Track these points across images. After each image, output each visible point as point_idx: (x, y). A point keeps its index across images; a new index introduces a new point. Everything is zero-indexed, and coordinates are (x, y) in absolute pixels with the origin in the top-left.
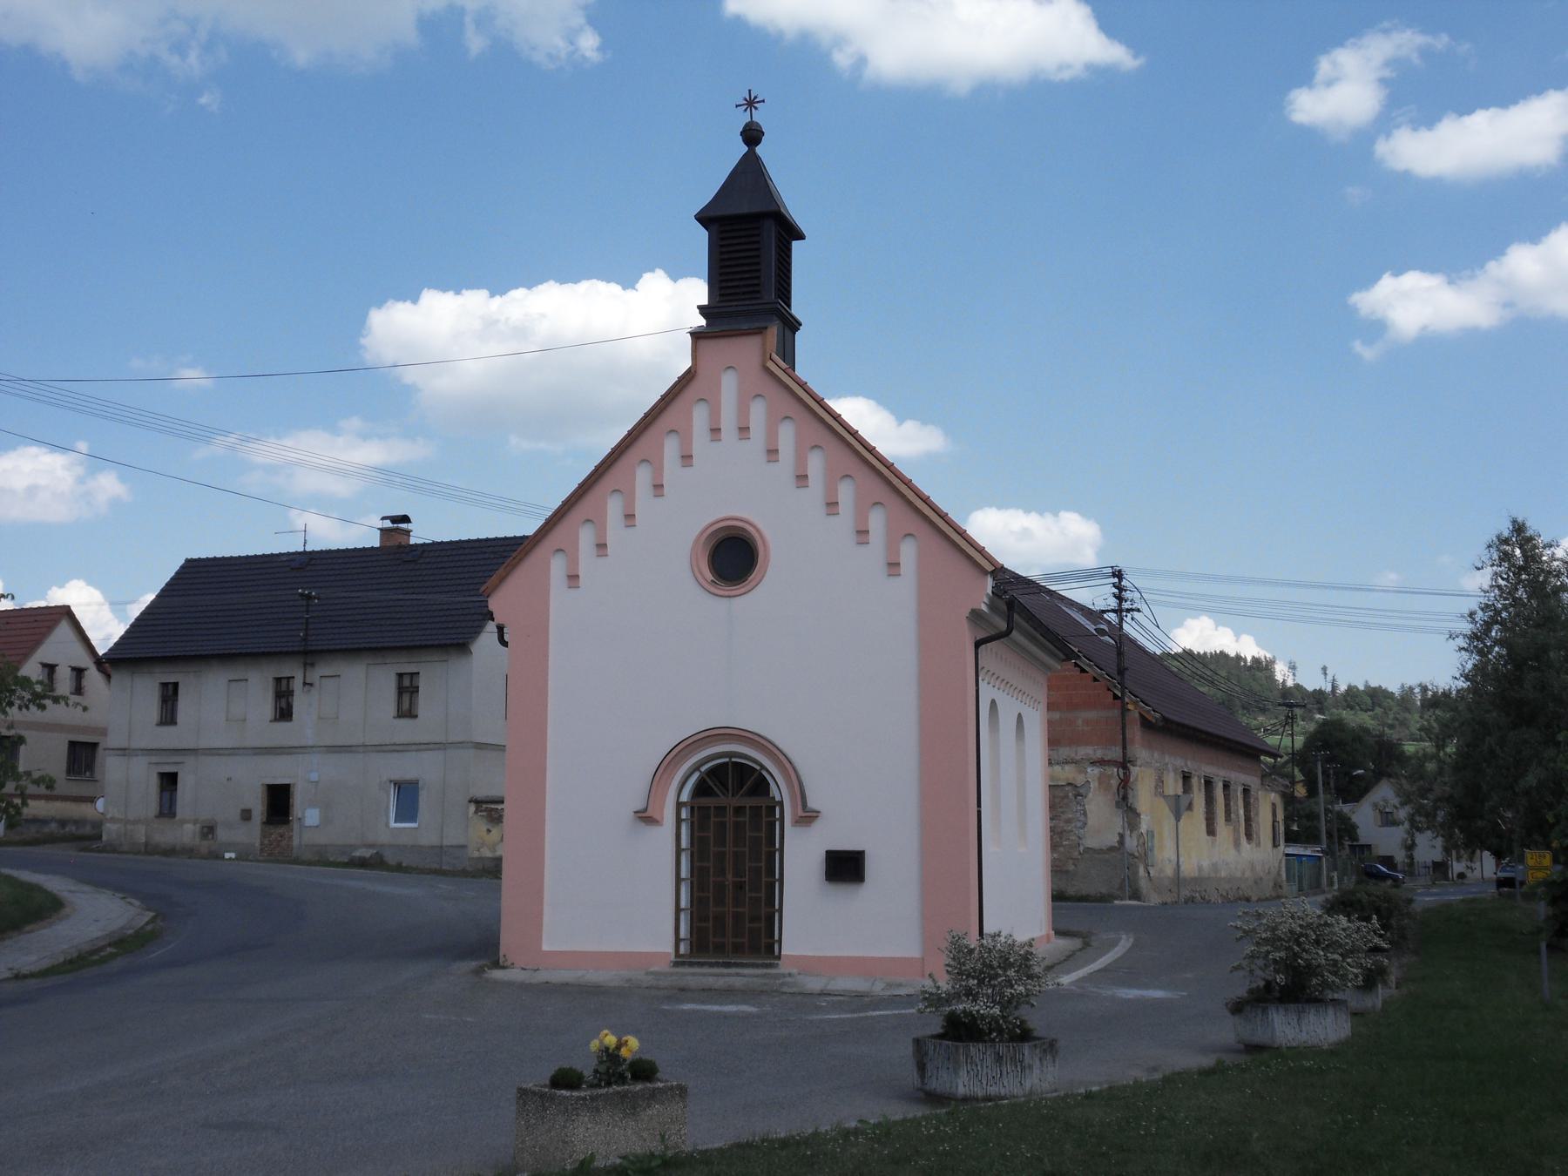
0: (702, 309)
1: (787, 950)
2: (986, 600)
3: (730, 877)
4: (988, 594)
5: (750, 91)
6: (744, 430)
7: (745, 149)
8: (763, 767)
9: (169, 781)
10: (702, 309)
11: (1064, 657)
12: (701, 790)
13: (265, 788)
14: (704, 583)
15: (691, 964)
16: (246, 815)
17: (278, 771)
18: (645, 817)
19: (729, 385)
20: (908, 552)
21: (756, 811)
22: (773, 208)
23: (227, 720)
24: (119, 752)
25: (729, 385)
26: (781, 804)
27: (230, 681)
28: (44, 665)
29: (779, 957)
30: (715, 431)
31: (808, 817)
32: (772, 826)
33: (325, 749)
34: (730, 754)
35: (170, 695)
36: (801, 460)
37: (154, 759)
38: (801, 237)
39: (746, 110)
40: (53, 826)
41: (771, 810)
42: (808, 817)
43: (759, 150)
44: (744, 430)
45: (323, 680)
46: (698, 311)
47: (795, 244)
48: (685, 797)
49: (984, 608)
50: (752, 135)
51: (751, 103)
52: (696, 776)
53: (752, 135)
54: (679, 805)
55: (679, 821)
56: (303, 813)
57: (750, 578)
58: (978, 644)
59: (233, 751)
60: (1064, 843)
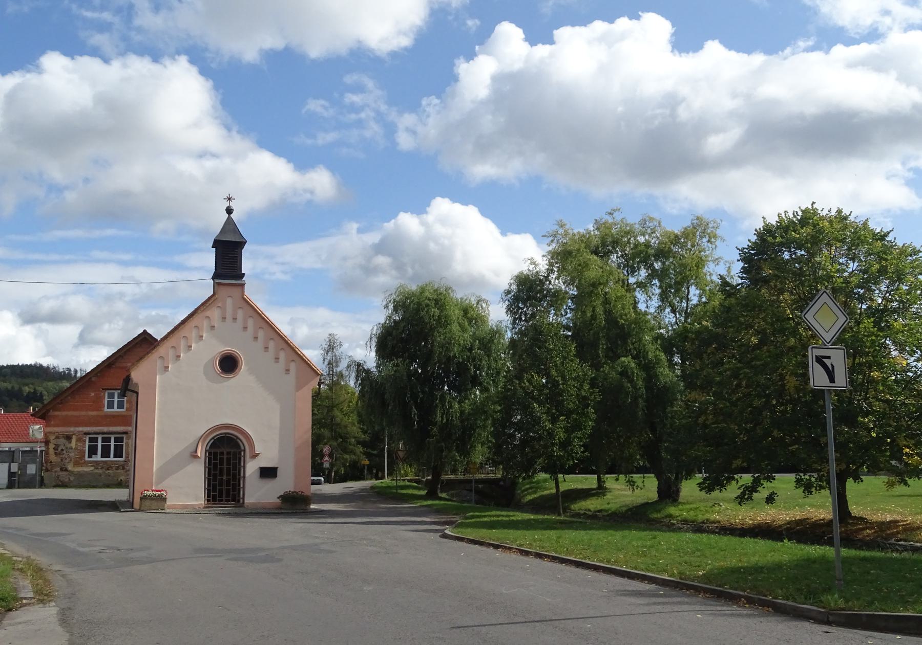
1: (248, 501)
6: (235, 319)
7: (227, 215)
8: (238, 438)
18: (194, 455)
20: (293, 366)
21: (235, 453)
25: (229, 301)
26: (244, 451)
29: (243, 503)
30: (224, 318)
31: (254, 456)
32: (240, 459)
41: (240, 453)
42: (254, 456)
43: (232, 216)
44: (235, 319)
48: (208, 448)
50: (229, 211)
51: (229, 199)
53: (229, 211)
54: (206, 451)
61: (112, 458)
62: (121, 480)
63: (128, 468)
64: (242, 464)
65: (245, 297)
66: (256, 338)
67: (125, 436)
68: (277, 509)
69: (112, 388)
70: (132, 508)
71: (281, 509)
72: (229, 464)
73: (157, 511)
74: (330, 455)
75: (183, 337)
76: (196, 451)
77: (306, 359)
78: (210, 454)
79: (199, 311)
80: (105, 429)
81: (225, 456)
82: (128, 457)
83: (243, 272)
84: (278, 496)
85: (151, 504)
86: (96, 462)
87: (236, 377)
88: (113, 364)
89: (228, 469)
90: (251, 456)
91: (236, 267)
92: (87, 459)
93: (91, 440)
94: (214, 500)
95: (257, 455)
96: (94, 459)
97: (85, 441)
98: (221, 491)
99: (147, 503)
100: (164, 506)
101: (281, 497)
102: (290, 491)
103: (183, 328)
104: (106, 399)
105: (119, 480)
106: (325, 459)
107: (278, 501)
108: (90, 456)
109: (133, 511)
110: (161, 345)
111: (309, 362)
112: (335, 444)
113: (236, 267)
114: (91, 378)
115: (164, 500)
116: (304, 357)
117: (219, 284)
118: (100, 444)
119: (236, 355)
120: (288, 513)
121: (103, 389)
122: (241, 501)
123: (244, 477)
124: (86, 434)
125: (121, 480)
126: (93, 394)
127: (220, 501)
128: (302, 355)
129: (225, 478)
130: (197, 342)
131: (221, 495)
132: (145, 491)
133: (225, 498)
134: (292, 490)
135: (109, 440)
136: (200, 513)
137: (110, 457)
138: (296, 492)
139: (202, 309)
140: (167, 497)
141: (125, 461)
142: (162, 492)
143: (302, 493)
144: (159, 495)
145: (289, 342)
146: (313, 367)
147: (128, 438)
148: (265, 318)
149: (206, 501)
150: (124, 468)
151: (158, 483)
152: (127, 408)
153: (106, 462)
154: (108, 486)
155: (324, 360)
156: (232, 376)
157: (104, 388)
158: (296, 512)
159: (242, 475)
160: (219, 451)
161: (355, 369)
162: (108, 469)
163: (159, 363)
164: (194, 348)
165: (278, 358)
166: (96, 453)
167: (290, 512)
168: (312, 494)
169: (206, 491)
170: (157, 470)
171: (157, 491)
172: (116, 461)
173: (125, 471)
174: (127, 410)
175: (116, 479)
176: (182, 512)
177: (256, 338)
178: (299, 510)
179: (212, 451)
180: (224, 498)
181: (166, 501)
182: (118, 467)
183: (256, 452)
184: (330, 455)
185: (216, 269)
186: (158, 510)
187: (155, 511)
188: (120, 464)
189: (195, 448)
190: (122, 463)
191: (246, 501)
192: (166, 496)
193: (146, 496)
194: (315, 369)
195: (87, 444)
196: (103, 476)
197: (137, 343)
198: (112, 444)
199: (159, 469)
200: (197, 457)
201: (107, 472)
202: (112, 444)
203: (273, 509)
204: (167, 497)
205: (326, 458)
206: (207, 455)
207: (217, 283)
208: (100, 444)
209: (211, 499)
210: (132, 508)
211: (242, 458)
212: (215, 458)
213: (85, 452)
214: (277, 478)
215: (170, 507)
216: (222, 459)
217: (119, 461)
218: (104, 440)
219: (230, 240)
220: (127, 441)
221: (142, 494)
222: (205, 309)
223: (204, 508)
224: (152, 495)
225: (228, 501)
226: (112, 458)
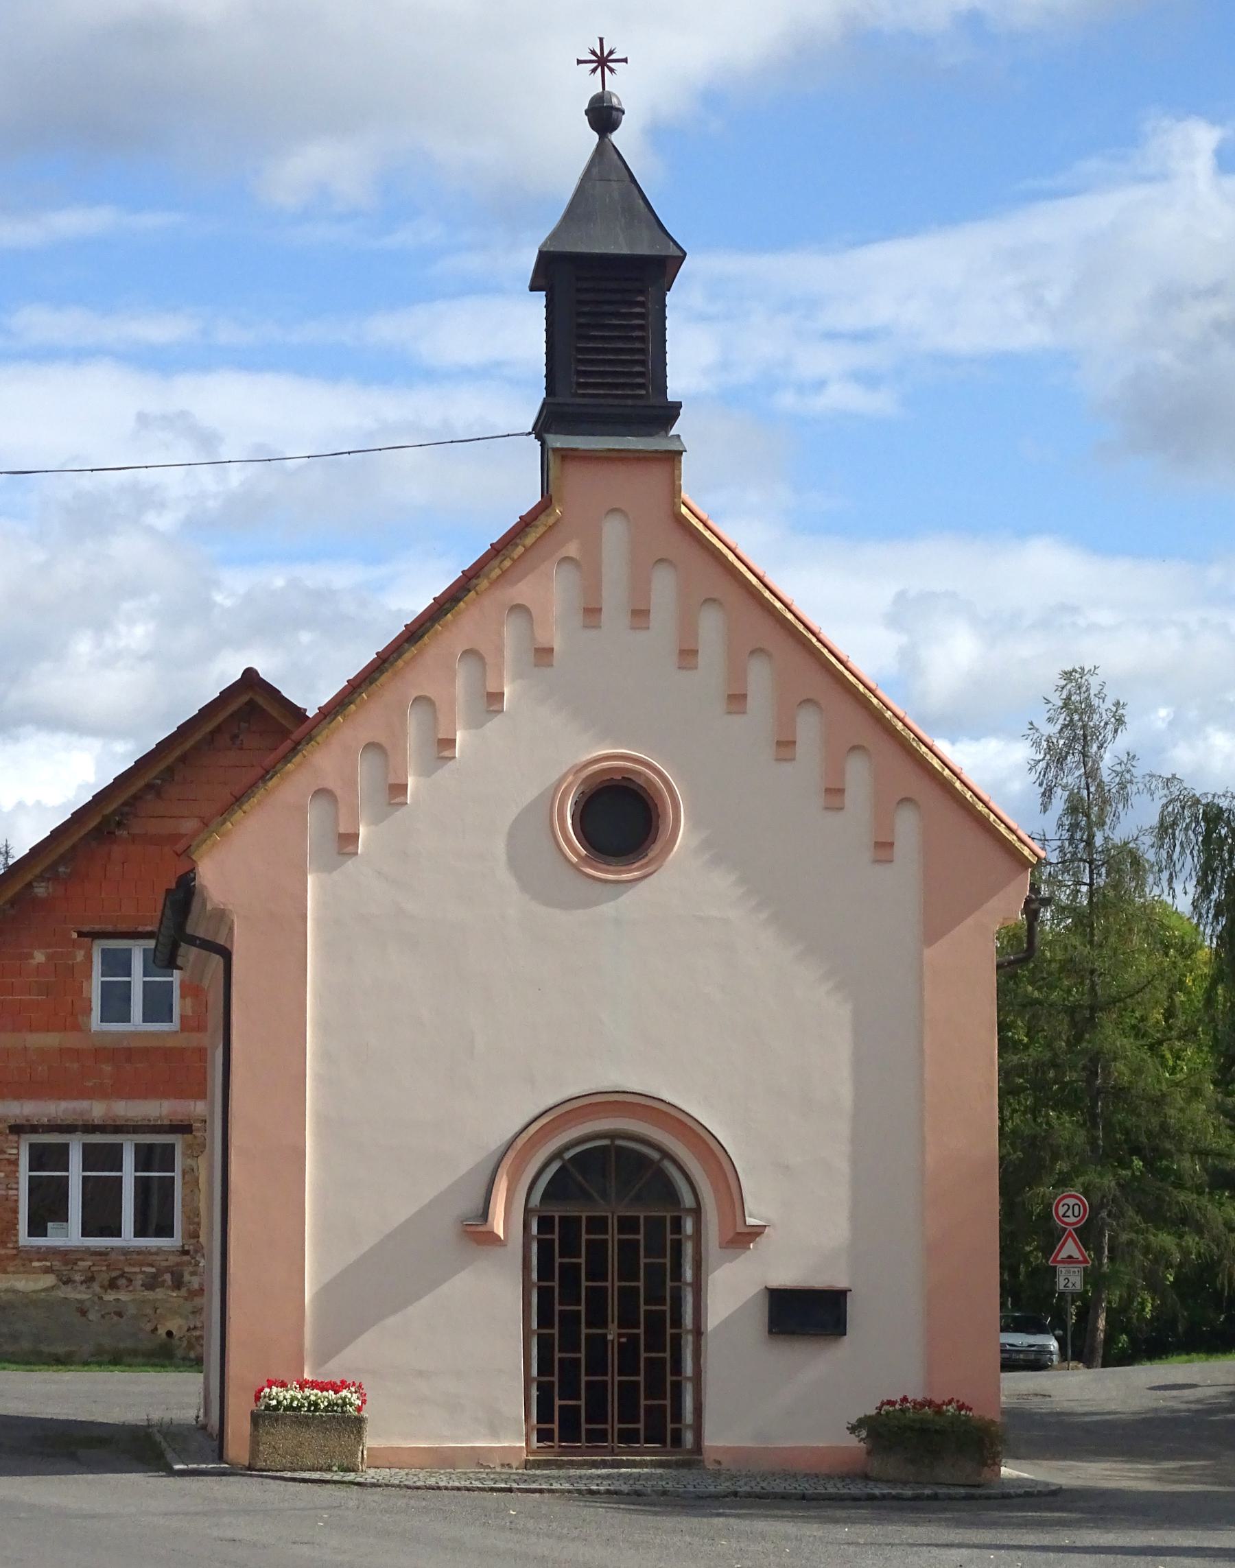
5: (601, 40)
6: (640, 615)
7: (595, 137)
8: (666, 1154)
12: (560, 1188)
14: (575, 860)
19: (614, 534)
20: (907, 827)
21: (655, 1225)
25: (614, 534)
26: (697, 1212)
30: (592, 613)
32: (677, 1248)
34: (612, 1135)
36: (736, 672)
39: (594, 70)
41: (677, 1225)
44: (640, 615)
51: (602, 61)
52: (555, 1166)
54: (527, 1211)
57: (651, 854)
61: (128, 1237)
62: (169, 1334)
63: (195, 1283)
64: (688, 1275)
65: (684, 510)
66: (737, 700)
67: (177, 1141)
69: (123, 927)
70: (221, 1458)
71: (866, 1477)
72: (628, 1270)
73: (328, 1476)
74: (1087, 1234)
75: (416, 699)
76: (485, 1214)
77: (969, 795)
78: (545, 1224)
79: (484, 583)
80: (97, 1110)
81: (613, 1237)
82: (195, 1235)
83: (671, 397)
84: (854, 1421)
85: (300, 1444)
86: (67, 1256)
87: (646, 881)
88: (119, 824)
89: (628, 1296)
90: (731, 1235)
91: (641, 374)
92: (24, 1239)
93: (40, 1157)
94: (570, 1431)
95: (755, 1233)
96: (54, 1238)
97: (15, 1163)
98: (597, 1393)
99: (282, 1438)
100: (353, 1454)
102: (905, 1399)
103: (414, 657)
104: (97, 979)
105: (162, 1332)
106: (1063, 1254)
107: (854, 1443)
108: (37, 1228)
109: (223, 1473)
110: (319, 739)
111: (980, 806)
112: (1109, 1182)
113: (641, 374)
114: (29, 885)
115: (356, 1424)
116: (958, 785)
117: (566, 455)
118: (75, 1174)
119: (648, 780)
120: (897, 1498)
121: (81, 934)
122: (688, 1437)
123: (698, 1332)
124: (17, 1129)
125: (169, 1334)
126: (39, 957)
128: (947, 772)
129: (612, 1333)
130: (475, 724)
131: (597, 1412)
132: (270, 1384)
133: (617, 1426)
134: (916, 1394)
135: (112, 1157)
136: (510, 1490)
137: (118, 1233)
138: (929, 1403)
139: (497, 572)
140: (364, 1414)
141: (186, 1253)
142: (344, 1393)
143: (961, 1407)
144: (331, 1404)
145: (888, 714)
146: (1002, 828)
147: (196, 1150)
148: (778, 605)
149: (534, 1437)
150: (178, 1284)
151: (323, 1358)
152: (182, 1017)
153: (102, 1253)
154: (115, 1359)
155: (1048, 794)
157: (86, 929)
158: (935, 1497)
159: (688, 1321)
160: (584, 1215)
161: (1196, 839)
162: (112, 1285)
163: (314, 816)
164: (462, 752)
165: (840, 791)
166: (63, 1217)
167: (909, 1492)
168: (1005, 1412)
169: (534, 1393)
170: (317, 1296)
171: (323, 1387)
172: (140, 1252)
173: (183, 1292)
174: (184, 1027)
175: (149, 1327)
176: (432, 1481)
179: (557, 1212)
180: (614, 1425)
181: (360, 1433)
182: (155, 1276)
183: (751, 1221)
184: (1087, 1234)
185: (550, 389)
186: (329, 1469)
187: (316, 1475)
188: (164, 1264)
190: (173, 1259)
191: (709, 1442)
192: (359, 1409)
193: (276, 1408)
194: (1012, 837)
195: (24, 1174)
196: (92, 1316)
197: (218, 729)
198: (128, 1174)
199: (327, 1292)
201: (110, 1296)
202: (128, 1174)
203: (829, 1477)
204: (364, 1414)
205: (1070, 1248)
206: (534, 1229)
207: (556, 450)
208: (75, 1174)
209: (555, 1426)
210: (221, 1458)
211: (688, 1248)
212: (570, 1247)
213: (15, 1211)
214: (845, 1337)
215: (380, 1458)
216: (596, 1250)
217: (159, 1251)
218: (92, 1157)
219: (613, 250)
220: (189, 1161)
221: (257, 1398)
222: (504, 573)
223: (527, 1464)
224: (299, 1408)
225: (628, 1437)
226: (128, 1237)
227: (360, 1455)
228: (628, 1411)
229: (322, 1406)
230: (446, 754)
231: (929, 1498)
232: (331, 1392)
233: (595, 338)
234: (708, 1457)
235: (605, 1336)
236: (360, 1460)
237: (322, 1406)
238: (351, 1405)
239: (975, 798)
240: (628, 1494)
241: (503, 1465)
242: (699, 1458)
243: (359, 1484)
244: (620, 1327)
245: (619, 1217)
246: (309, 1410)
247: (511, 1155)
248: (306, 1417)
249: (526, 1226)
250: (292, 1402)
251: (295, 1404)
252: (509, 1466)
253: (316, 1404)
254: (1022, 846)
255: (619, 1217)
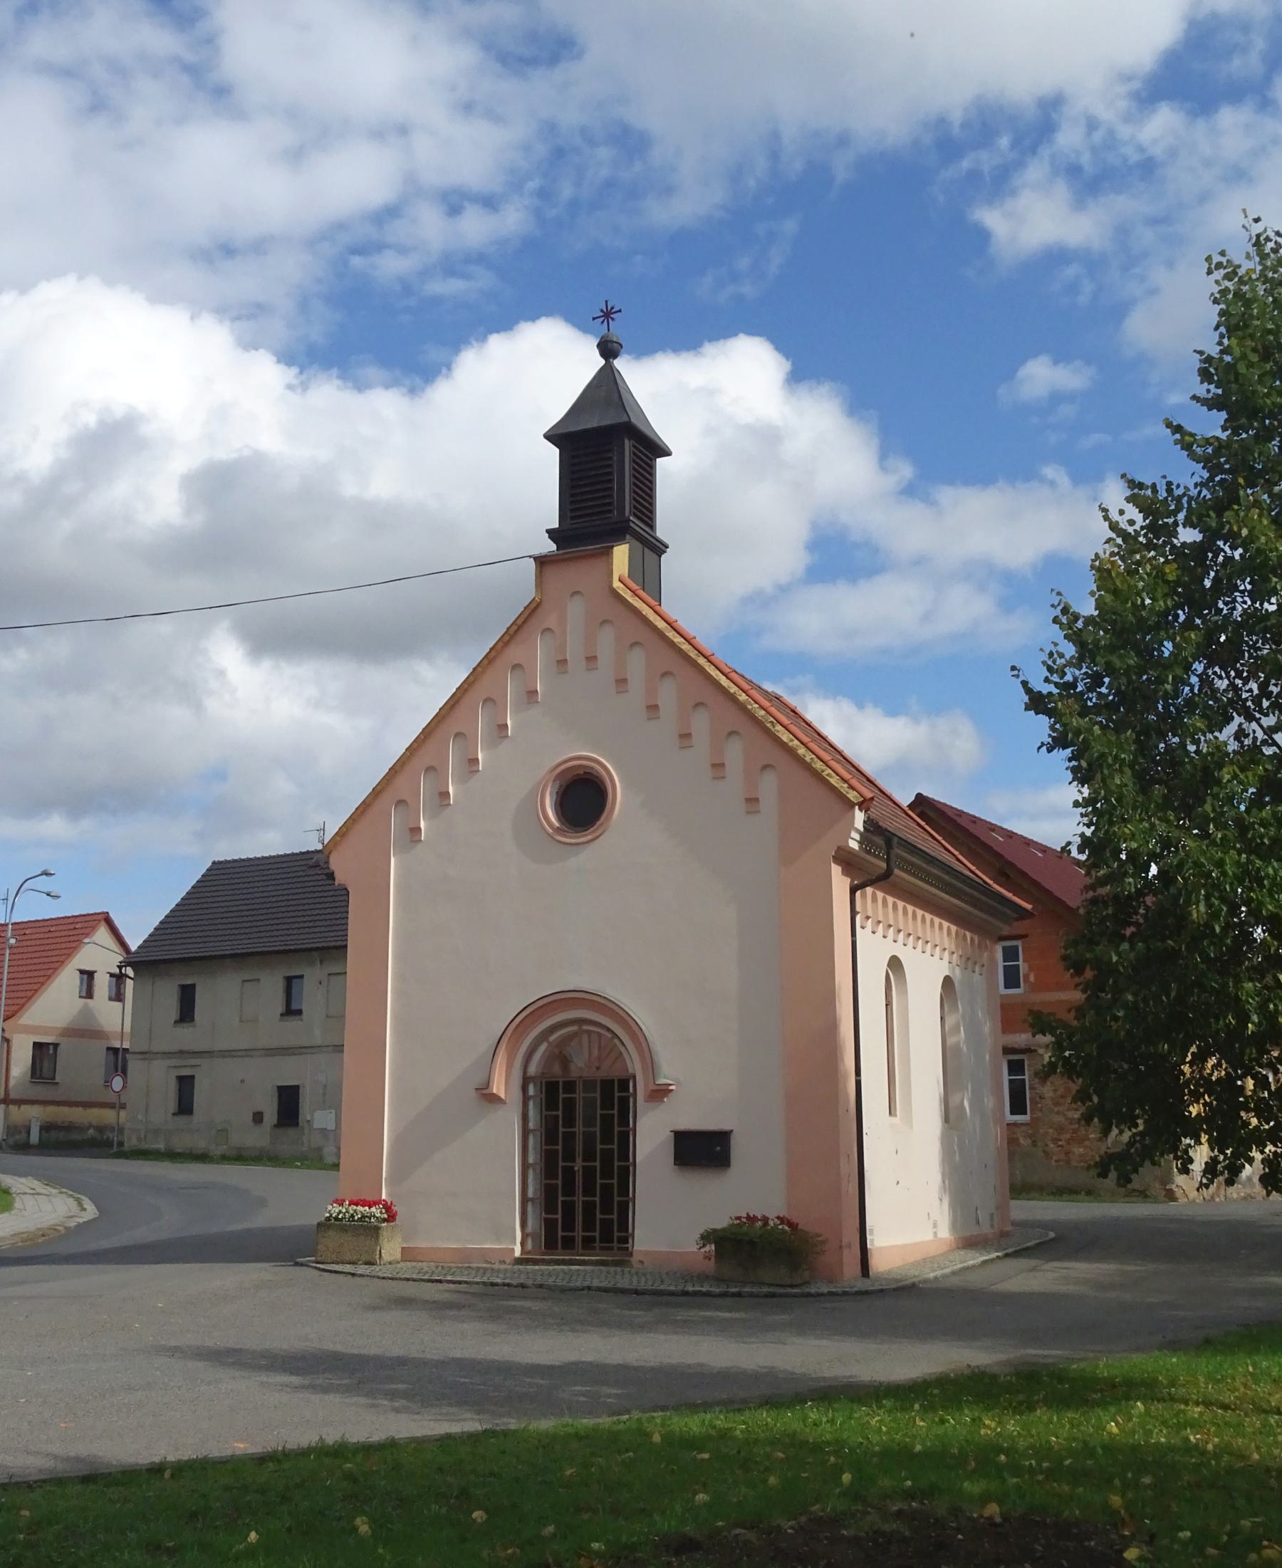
0: (552, 533)
2: (857, 837)
3: (578, 1165)
4: (857, 831)
6: (591, 659)
9: (185, 1085)
10: (552, 533)
11: (1015, 915)
13: (276, 1089)
14: (551, 831)
15: (535, 1262)
16: (258, 1117)
17: (288, 1072)
19: (576, 610)
20: (768, 786)
21: (607, 1085)
22: (625, 419)
23: (241, 1021)
24: (140, 1056)
26: (634, 1077)
27: (244, 981)
28: (82, 972)
29: (631, 1255)
31: (659, 1093)
33: (331, 1048)
35: (187, 999)
37: (174, 1062)
38: (666, 453)
40: (91, 1131)
42: (659, 1093)
44: (591, 659)
45: (332, 978)
46: (547, 535)
47: (660, 462)
49: (854, 845)
52: (544, 1047)
55: (526, 1099)
56: (312, 1116)
57: (598, 823)
58: (853, 891)
59: (248, 1053)
60: (1091, 1136)
68: (689, 1277)
75: (457, 735)
76: (488, 1084)
85: (341, 1245)
101: (706, 1237)
113: (610, 504)
127: (569, 1244)
129: (578, 1165)
131: (569, 1224)
142: (373, 1209)
144: (363, 1216)
156: (590, 837)
158: (739, 1295)
167: (716, 1290)
177: (653, 708)
178: (770, 1285)
181: (377, 1237)
183: (662, 1081)
189: (487, 1075)
193: (328, 1219)
200: (493, 1099)
216: (570, 1105)
219: (589, 426)
225: (588, 1243)
227: (378, 1253)
228: (589, 1225)
229: (356, 1218)
230: (474, 768)
231: (734, 1295)
232: (367, 1208)
233: (585, 485)
234: (634, 1260)
235: (573, 1167)
236: (378, 1256)
237: (356, 1218)
238: (374, 1216)
239: (816, 759)
240: (516, 1286)
241: (500, 1262)
242: (627, 1258)
243: (353, 1275)
244: (584, 1160)
245: (584, 1081)
246: (349, 1221)
247: (505, 1039)
248: (346, 1225)
249: (524, 1089)
250: (338, 1214)
251: (340, 1217)
252: (504, 1262)
253: (352, 1216)
254: (851, 791)
255: (584, 1081)
